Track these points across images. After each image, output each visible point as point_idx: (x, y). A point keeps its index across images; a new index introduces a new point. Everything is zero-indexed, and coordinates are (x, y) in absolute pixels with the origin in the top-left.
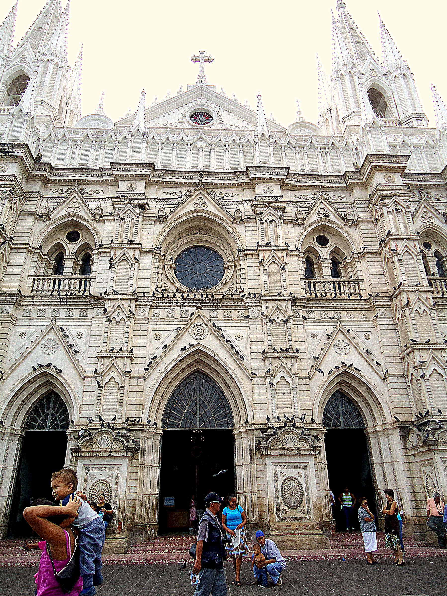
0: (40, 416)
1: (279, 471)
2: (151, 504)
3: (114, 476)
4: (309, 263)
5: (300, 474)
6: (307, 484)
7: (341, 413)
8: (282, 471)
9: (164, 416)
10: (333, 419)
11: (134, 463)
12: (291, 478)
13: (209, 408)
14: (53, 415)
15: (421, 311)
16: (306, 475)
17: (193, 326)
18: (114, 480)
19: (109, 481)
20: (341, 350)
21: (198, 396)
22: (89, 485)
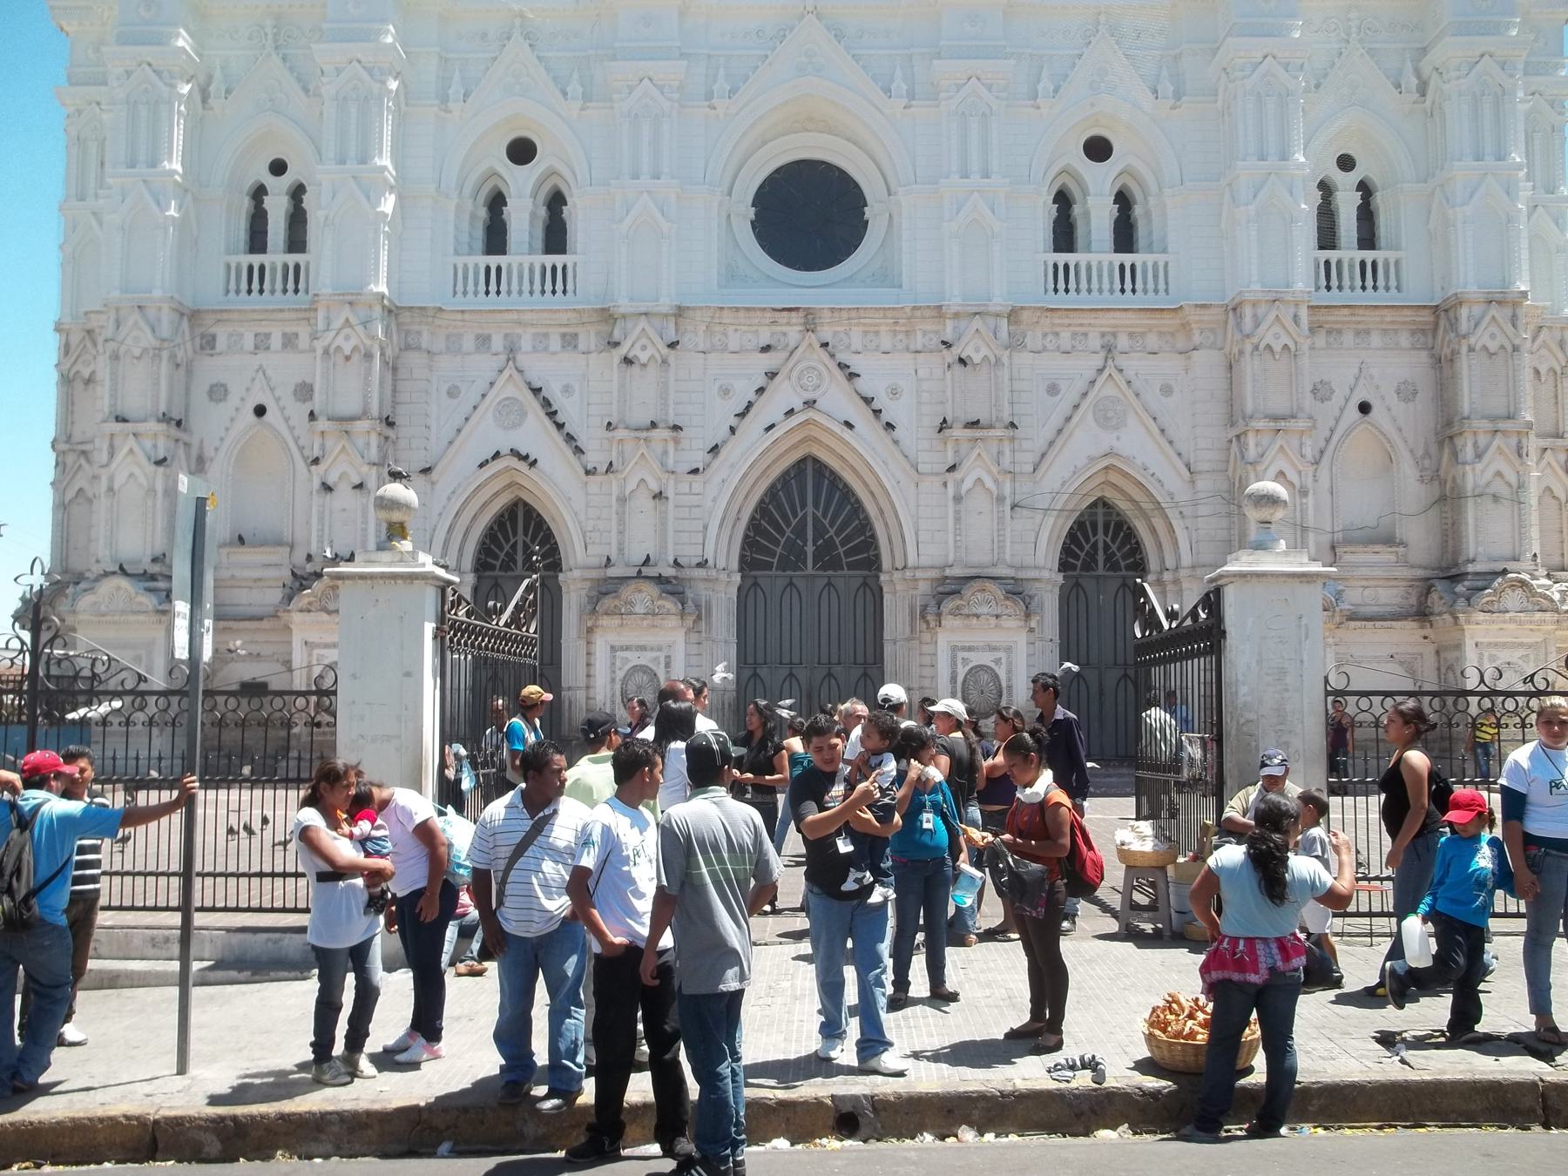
0: (501, 548)
1: (961, 655)
2: (726, 706)
3: (662, 660)
4: (1063, 200)
5: (997, 661)
6: (1009, 680)
7: (1101, 545)
8: (966, 654)
9: (743, 549)
10: (1082, 555)
11: (694, 637)
12: (981, 667)
13: (832, 532)
14: (526, 547)
15: (1277, 348)
16: (1010, 664)
17: (800, 366)
18: (662, 665)
19: (654, 668)
20: (1108, 419)
21: (810, 508)
22: (620, 675)
